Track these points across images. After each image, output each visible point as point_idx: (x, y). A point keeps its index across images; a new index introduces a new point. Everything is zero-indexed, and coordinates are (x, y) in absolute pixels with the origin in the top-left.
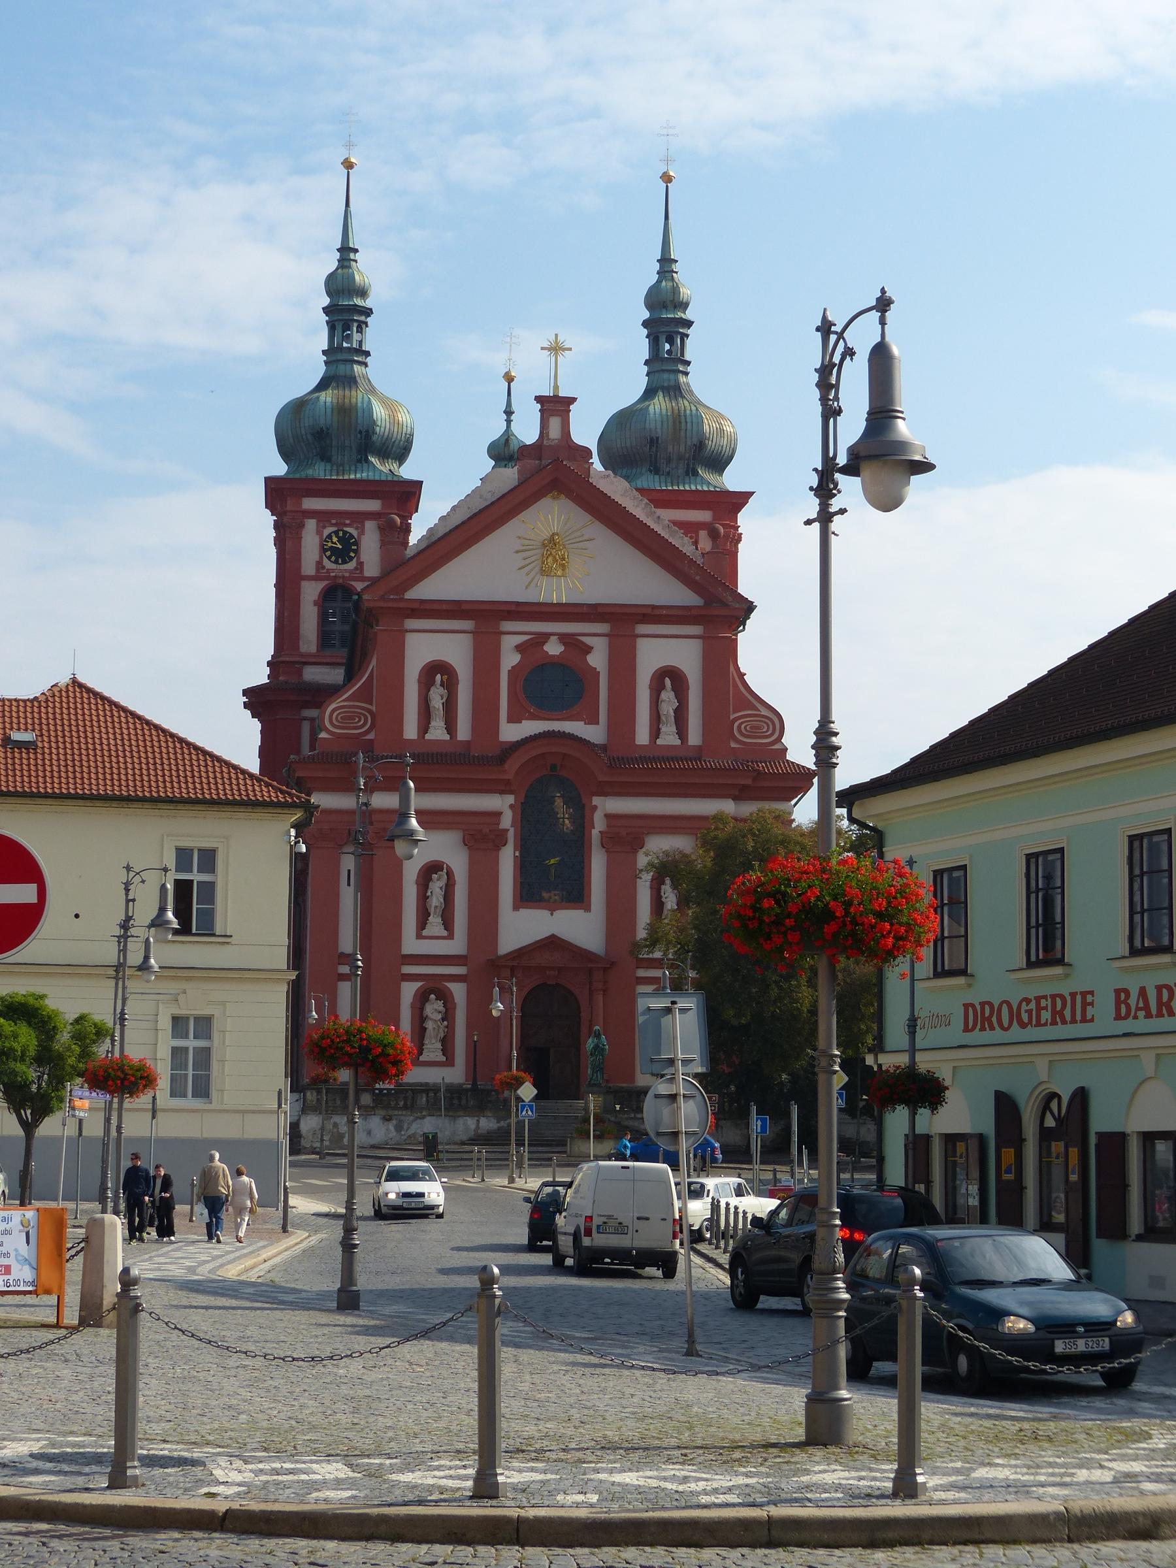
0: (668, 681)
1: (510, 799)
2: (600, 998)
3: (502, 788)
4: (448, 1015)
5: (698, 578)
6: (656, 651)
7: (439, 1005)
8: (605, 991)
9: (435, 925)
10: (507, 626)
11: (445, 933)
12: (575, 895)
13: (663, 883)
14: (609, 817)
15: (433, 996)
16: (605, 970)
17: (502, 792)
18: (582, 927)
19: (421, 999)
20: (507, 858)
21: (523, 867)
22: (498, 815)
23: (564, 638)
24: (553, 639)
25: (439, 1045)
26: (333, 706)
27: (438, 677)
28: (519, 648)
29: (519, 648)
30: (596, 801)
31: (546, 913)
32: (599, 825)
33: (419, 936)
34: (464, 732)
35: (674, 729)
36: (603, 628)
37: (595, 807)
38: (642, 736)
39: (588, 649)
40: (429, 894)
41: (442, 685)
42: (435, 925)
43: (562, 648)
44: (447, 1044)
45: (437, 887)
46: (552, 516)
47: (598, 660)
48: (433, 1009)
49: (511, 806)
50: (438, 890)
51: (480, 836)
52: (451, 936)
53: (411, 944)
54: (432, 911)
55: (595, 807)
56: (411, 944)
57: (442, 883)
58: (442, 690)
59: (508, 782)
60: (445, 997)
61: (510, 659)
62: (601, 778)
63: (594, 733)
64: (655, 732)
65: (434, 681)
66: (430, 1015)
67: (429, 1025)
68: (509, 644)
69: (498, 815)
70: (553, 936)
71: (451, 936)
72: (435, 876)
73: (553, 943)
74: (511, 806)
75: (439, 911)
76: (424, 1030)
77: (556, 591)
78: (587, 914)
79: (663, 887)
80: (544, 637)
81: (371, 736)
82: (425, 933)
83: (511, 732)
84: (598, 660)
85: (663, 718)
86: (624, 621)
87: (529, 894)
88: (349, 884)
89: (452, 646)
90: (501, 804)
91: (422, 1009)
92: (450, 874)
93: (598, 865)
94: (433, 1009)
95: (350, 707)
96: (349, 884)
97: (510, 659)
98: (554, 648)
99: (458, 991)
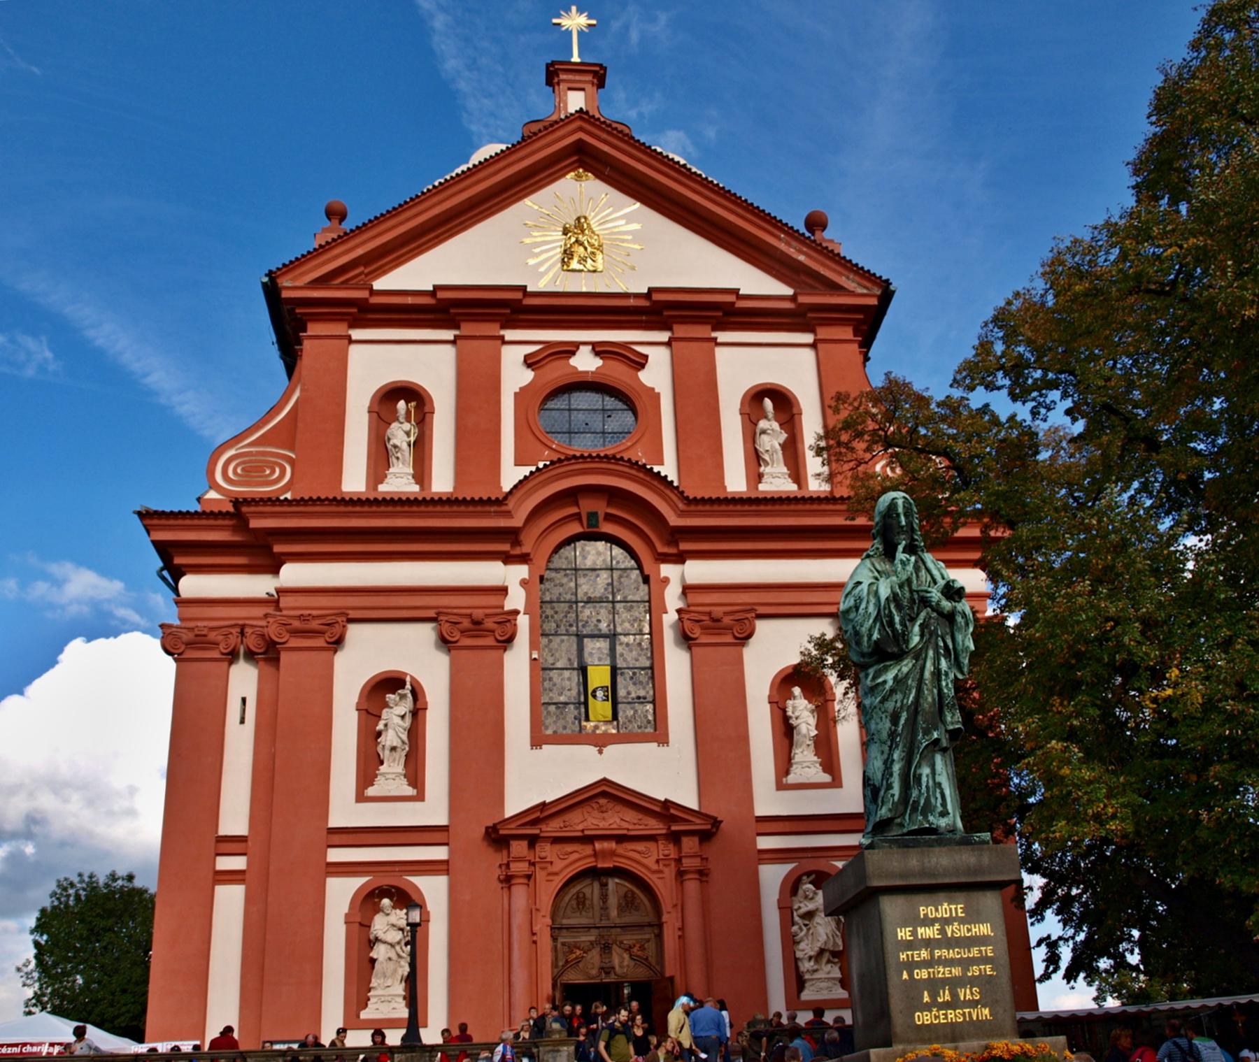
0: (768, 403)
1: (522, 571)
2: (692, 886)
3: (504, 544)
4: (415, 935)
5: (802, 258)
7: (399, 917)
8: (703, 874)
9: (391, 777)
10: (510, 335)
11: (410, 791)
13: (791, 696)
14: (687, 590)
15: (386, 902)
16: (705, 836)
17: (508, 559)
19: (368, 902)
22: (503, 591)
23: (599, 350)
24: (585, 351)
25: (400, 989)
26: (232, 452)
27: (401, 405)
28: (530, 362)
29: (530, 362)
30: (667, 570)
31: (594, 750)
33: (361, 797)
35: (785, 470)
36: (664, 336)
37: (666, 581)
39: (640, 362)
40: (380, 727)
41: (408, 419)
42: (391, 777)
43: (599, 362)
45: (396, 713)
47: (657, 374)
49: (524, 583)
50: (398, 720)
52: (420, 797)
53: (344, 810)
54: (386, 755)
55: (666, 581)
56: (344, 810)
57: (405, 706)
58: (407, 426)
59: (512, 535)
60: (406, 899)
62: (674, 520)
64: (755, 477)
65: (396, 411)
66: (381, 935)
67: (380, 952)
69: (503, 591)
70: (605, 781)
71: (420, 797)
72: (390, 697)
73: (605, 793)
74: (524, 583)
75: (401, 756)
76: (373, 961)
78: (663, 750)
79: (790, 703)
80: (570, 349)
81: (289, 496)
82: (370, 792)
84: (657, 374)
85: (766, 457)
88: (242, 721)
91: (366, 926)
92: (417, 693)
94: (388, 923)
95: (259, 453)
96: (242, 721)
98: (585, 362)
99: (434, 890)
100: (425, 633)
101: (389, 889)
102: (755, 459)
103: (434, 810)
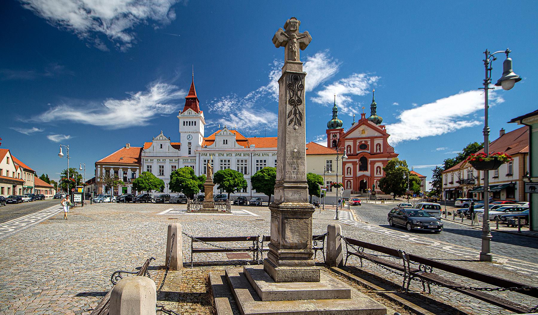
3: (357, 158)
6: (376, 142)
9: (349, 174)
12: (366, 169)
18: (368, 173)
19: (347, 182)
20: (358, 166)
21: (360, 167)
32: (369, 162)
34: (352, 153)
38: (375, 152)
42: (349, 174)
44: (350, 187)
45: (349, 169)
46: (363, 127)
47: (369, 143)
48: (349, 183)
51: (354, 163)
53: (346, 176)
61: (358, 144)
63: (369, 152)
68: (358, 142)
73: (364, 175)
77: (364, 136)
83: (358, 152)
84: (369, 143)
86: (372, 138)
87: (360, 170)
89: (351, 143)
90: (357, 160)
93: (369, 166)
94: (349, 183)
97: (358, 144)
98: (363, 142)
99: (352, 181)
100: (351, 164)
101: (349, 181)
102: (377, 149)
103: (352, 176)
